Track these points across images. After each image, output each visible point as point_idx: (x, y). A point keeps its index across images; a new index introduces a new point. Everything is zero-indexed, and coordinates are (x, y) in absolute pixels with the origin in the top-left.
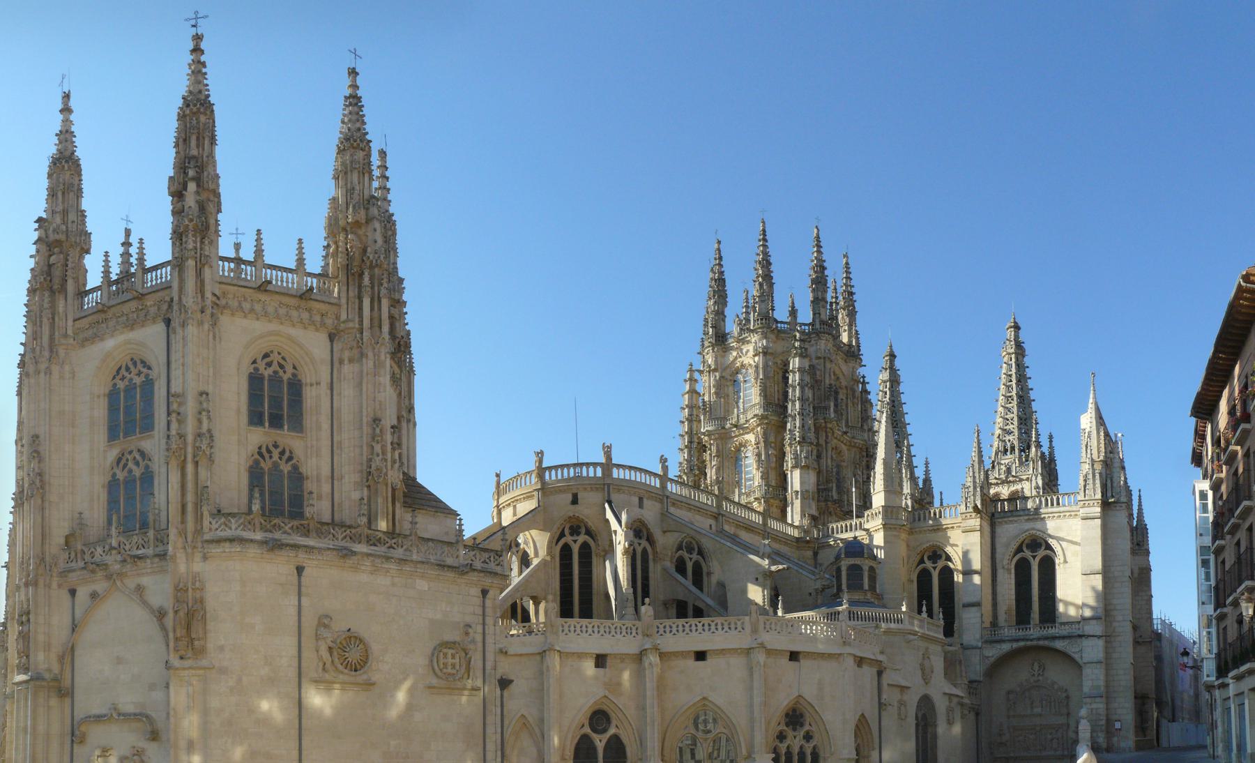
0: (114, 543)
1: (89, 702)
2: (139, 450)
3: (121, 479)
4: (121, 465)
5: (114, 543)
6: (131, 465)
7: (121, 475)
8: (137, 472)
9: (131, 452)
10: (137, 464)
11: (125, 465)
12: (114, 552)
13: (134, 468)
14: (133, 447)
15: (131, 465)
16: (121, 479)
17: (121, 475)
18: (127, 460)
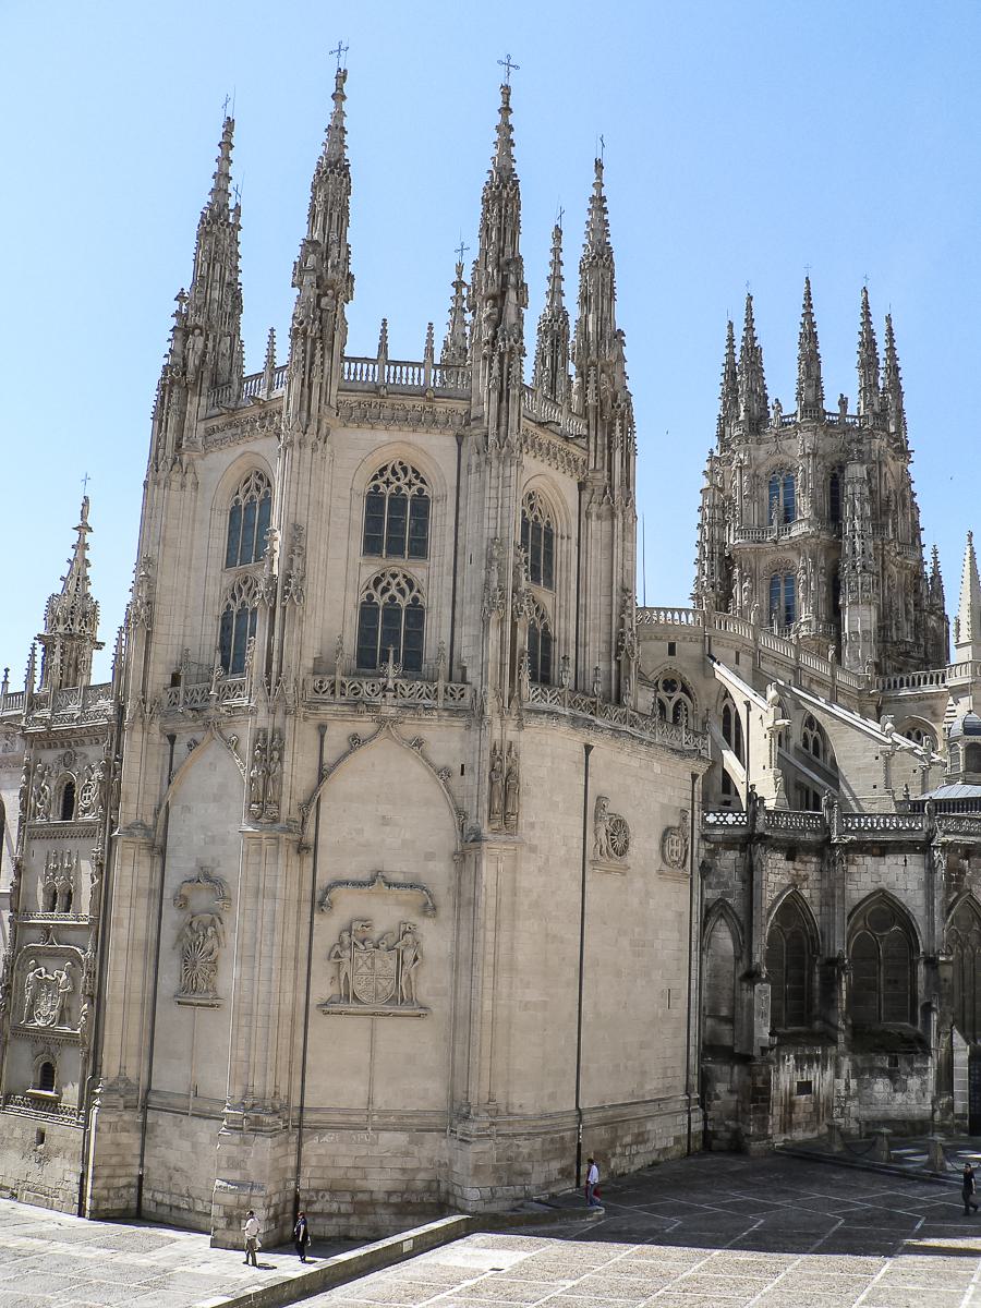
0: (391, 685)
1: (329, 868)
2: (405, 576)
3: (381, 604)
4: (380, 588)
5: (391, 685)
6: (393, 591)
7: (381, 600)
8: (403, 602)
9: (394, 576)
10: (402, 591)
11: (385, 590)
12: (390, 695)
13: (398, 596)
14: (395, 570)
15: (393, 591)
16: (381, 604)
17: (381, 600)
18: (389, 584)
